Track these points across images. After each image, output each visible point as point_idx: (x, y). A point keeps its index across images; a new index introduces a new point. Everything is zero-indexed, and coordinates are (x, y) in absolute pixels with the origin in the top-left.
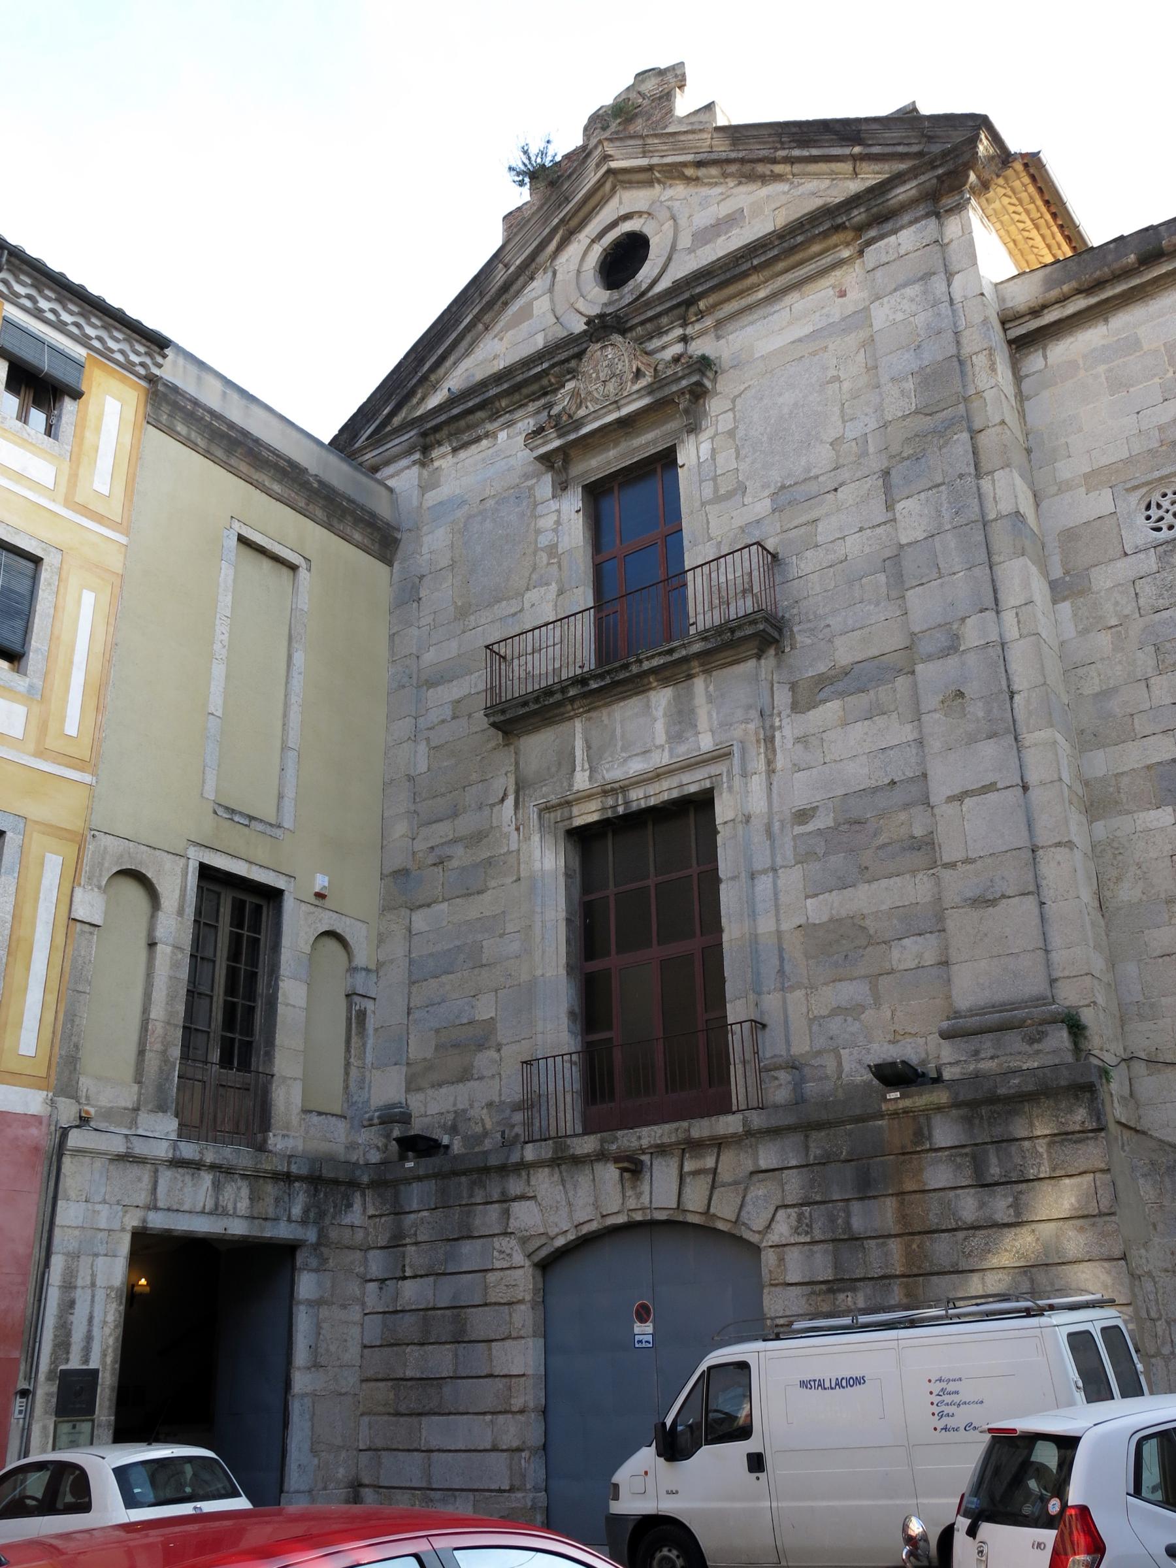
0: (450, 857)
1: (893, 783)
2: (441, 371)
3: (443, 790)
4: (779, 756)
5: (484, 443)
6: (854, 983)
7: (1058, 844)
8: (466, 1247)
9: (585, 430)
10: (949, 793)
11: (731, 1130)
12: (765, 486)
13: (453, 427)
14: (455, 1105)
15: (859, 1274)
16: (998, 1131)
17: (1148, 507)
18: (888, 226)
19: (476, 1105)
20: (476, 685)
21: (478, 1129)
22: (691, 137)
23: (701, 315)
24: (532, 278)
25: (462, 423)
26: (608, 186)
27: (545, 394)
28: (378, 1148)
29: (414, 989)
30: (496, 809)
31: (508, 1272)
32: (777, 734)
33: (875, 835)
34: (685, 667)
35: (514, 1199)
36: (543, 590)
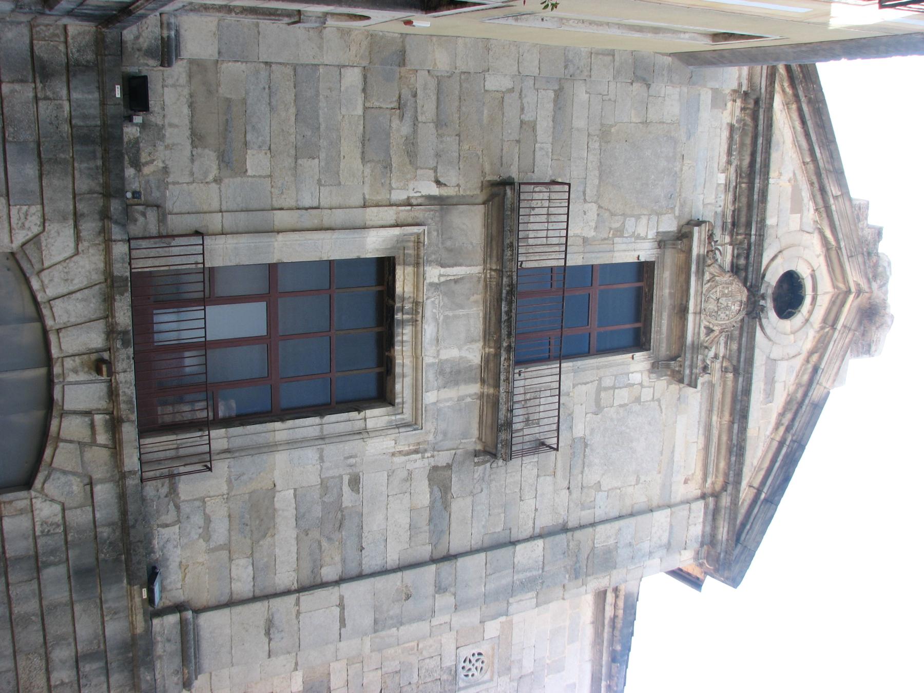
0: (402, 117)
1: (362, 549)
2: (795, 116)
3: (463, 109)
4: (403, 458)
5: (724, 158)
6: (226, 533)
7: (296, 664)
8: (31, 170)
9: (693, 279)
10: (346, 597)
11: (126, 461)
12: (592, 431)
13: (750, 129)
14: (171, 125)
15: (12, 579)
16: (114, 665)
17: (480, 654)
18: (710, 517)
19: (168, 152)
20: (541, 149)
21: (144, 157)
22: (835, 370)
23: (725, 370)
24: (817, 210)
25: (748, 141)
26: (841, 285)
27: (733, 224)
28: (137, 38)
29: (289, 71)
30: (431, 173)
31: (6, 225)
32: (419, 455)
33: (330, 539)
34: (491, 382)
35: (76, 226)
36: (593, 224)
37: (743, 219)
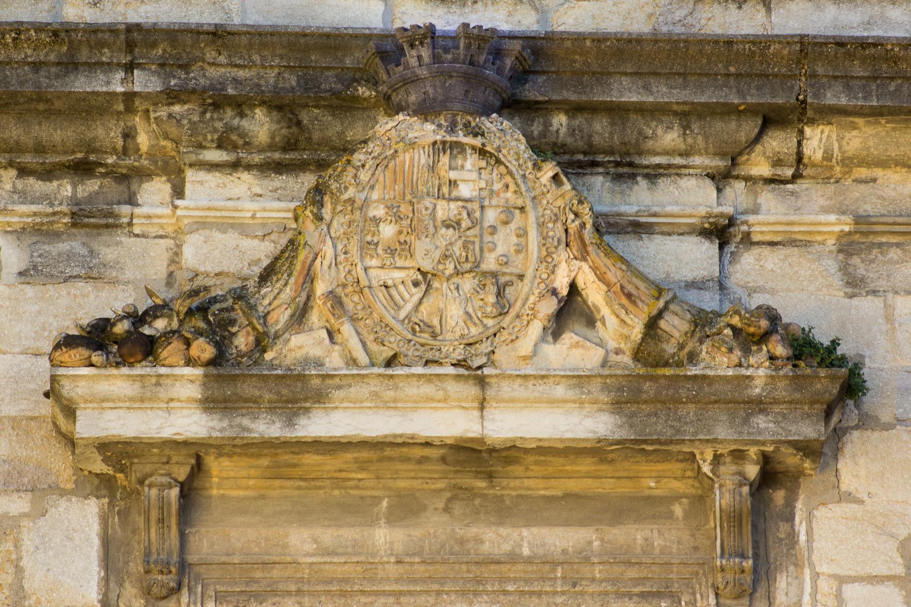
9: (318, 425)
27: (83, 169)
37: (60, 134)
